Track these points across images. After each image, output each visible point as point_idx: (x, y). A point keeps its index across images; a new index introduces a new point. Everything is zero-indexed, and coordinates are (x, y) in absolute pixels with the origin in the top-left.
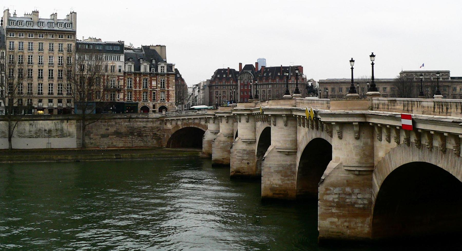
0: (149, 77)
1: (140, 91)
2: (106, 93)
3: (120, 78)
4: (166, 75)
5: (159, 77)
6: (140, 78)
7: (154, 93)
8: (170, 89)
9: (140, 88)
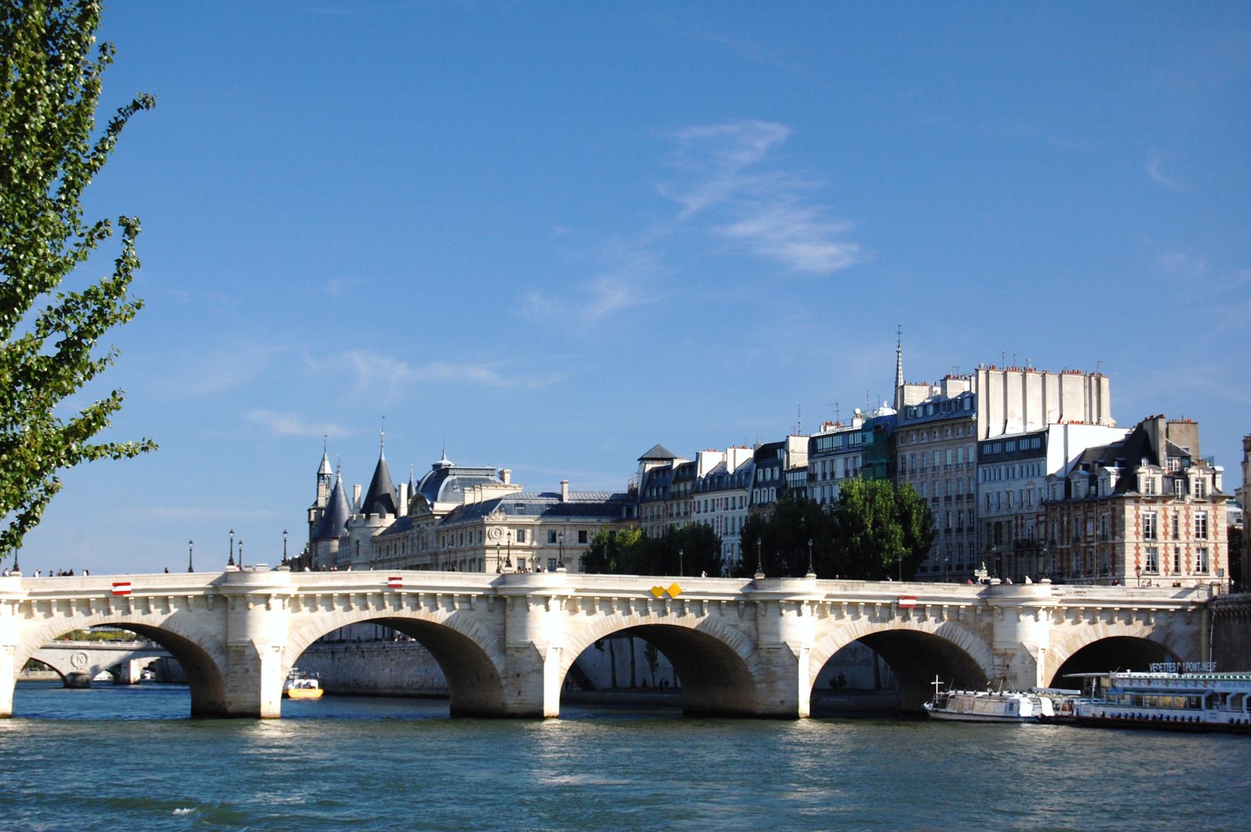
0: (1082, 512)
1: (1068, 549)
2: (1019, 559)
3: (1042, 518)
4: (1109, 502)
5: (1099, 511)
6: (1069, 515)
7: (1091, 553)
8: (1117, 538)
9: (1068, 544)
